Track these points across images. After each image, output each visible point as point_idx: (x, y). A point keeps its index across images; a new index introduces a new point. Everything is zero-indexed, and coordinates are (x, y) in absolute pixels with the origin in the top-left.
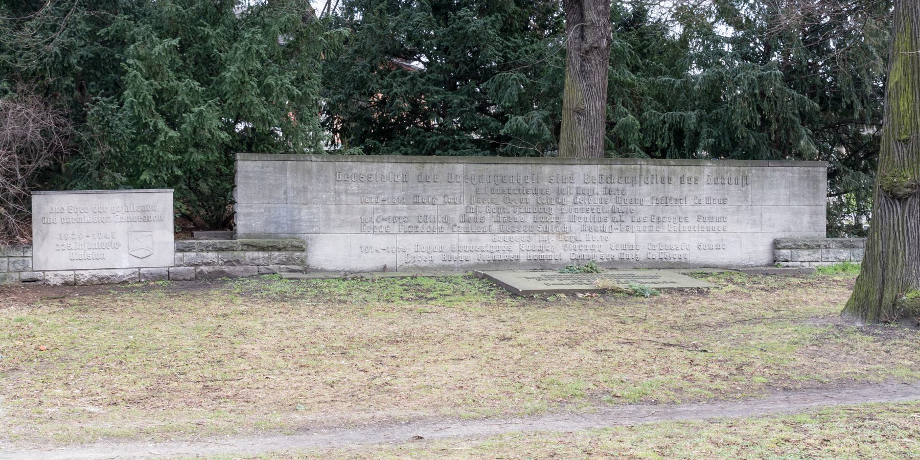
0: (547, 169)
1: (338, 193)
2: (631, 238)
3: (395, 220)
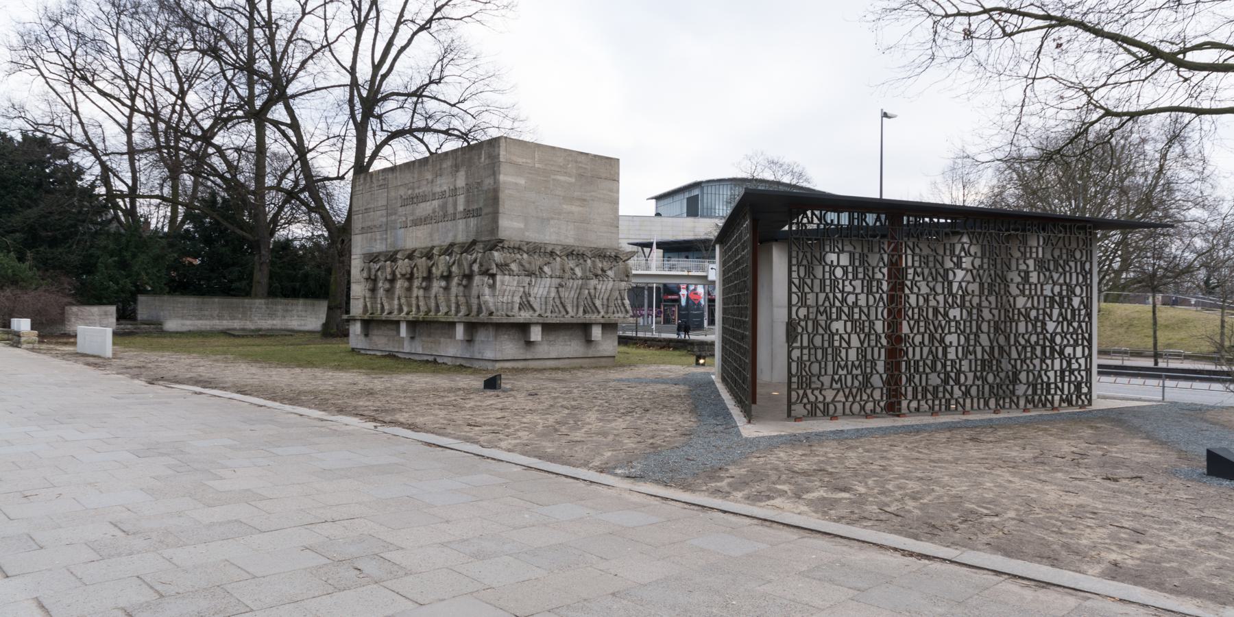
0: (246, 301)
1: (174, 307)
2: (275, 322)
3: (193, 316)
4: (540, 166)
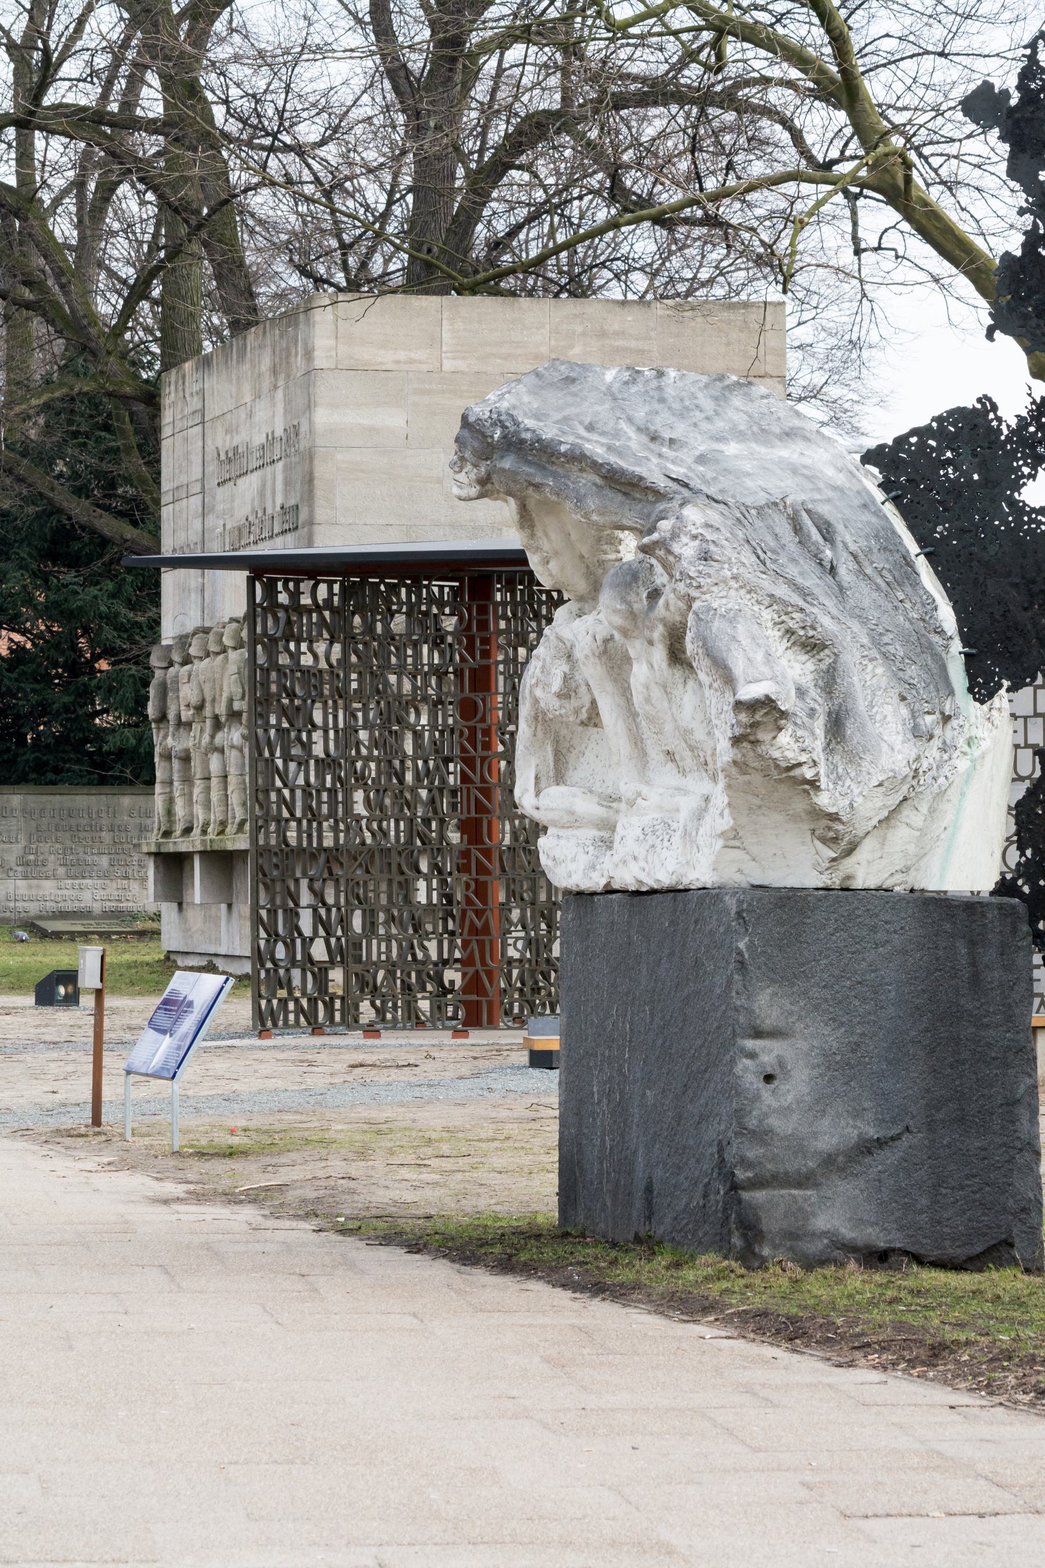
4: (461, 365)
